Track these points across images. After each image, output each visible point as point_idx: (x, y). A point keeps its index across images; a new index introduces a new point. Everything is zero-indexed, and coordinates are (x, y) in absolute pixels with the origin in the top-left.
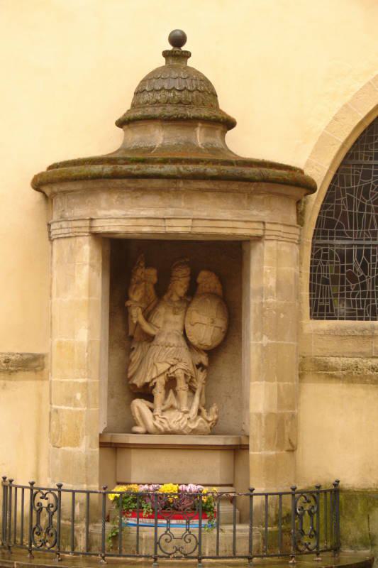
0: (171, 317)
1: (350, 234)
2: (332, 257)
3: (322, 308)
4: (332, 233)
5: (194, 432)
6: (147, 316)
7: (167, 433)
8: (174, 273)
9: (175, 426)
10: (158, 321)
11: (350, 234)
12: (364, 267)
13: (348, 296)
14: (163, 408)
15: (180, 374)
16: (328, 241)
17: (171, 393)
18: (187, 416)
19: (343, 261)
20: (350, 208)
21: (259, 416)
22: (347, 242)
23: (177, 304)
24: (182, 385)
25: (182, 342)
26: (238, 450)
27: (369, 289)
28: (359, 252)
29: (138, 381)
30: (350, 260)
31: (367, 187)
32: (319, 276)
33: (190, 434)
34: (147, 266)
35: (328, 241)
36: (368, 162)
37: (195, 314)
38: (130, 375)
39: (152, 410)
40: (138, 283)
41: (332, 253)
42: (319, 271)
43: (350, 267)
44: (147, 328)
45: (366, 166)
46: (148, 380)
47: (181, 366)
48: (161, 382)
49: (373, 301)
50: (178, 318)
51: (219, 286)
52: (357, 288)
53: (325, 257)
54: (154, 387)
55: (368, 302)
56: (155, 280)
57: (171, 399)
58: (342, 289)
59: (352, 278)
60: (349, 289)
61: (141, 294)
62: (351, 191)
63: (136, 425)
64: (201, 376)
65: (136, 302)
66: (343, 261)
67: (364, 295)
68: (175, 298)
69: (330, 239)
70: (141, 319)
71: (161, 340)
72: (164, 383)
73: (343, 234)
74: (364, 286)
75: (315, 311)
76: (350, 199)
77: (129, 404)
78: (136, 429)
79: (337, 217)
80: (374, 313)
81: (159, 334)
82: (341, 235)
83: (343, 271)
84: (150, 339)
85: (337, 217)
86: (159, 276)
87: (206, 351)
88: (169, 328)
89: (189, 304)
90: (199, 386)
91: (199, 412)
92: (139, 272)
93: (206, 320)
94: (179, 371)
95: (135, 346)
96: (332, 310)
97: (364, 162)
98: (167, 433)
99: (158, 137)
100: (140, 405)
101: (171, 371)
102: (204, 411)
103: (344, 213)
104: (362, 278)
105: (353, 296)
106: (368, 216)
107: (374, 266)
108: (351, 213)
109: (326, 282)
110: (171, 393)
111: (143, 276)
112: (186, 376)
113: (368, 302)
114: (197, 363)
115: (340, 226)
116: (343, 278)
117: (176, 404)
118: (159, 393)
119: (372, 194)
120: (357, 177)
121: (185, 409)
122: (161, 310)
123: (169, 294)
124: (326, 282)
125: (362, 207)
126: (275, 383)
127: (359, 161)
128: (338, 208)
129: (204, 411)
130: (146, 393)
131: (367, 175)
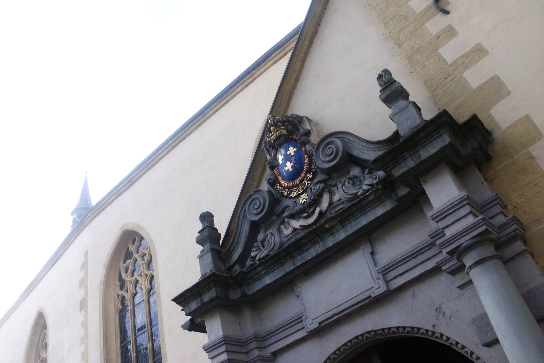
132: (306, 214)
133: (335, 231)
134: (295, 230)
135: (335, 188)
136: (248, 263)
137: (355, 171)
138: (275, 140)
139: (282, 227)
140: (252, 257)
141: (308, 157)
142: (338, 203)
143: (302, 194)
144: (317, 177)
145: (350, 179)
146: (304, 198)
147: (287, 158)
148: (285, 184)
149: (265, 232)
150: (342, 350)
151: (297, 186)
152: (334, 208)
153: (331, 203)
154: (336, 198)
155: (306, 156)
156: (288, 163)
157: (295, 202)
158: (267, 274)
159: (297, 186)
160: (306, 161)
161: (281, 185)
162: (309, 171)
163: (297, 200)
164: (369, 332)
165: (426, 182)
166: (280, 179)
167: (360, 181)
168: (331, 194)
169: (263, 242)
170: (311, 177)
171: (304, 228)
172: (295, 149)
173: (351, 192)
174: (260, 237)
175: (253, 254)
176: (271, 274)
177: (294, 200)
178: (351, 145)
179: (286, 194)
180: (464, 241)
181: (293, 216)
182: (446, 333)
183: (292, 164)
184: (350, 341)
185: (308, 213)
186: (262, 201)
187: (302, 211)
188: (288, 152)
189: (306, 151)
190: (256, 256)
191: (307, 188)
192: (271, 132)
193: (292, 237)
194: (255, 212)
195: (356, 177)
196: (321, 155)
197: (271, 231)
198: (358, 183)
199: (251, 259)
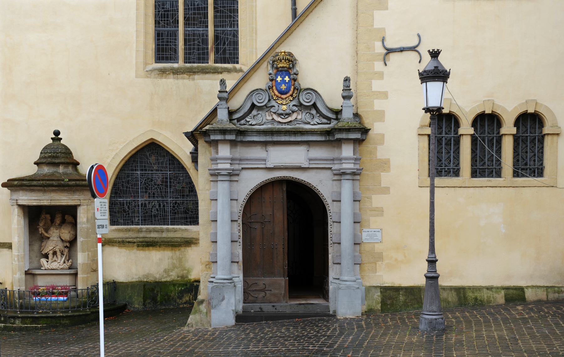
0: (55, 231)
1: (123, 196)
2: (117, 205)
3: (114, 222)
4: (117, 196)
5: (62, 269)
6: (47, 231)
7: (52, 269)
8: (56, 216)
9: (54, 267)
10: (51, 232)
11: (123, 196)
12: (129, 208)
13: (123, 217)
14: (52, 261)
15: (57, 250)
16: (116, 199)
17: (55, 256)
18: (59, 264)
19: (121, 206)
20: (123, 188)
21: (80, 264)
22: (122, 199)
23: (57, 227)
24: (59, 254)
25: (59, 239)
26: (76, 275)
27: (130, 215)
28: (127, 202)
29: (43, 252)
30: (123, 205)
31: (128, 181)
32: (113, 211)
33: (60, 269)
34: (46, 214)
35: (116, 199)
36: (129, 172)
37: (62, 230)
38: (41, 250)
39: (47, 262)
40: (42, 220)
41: (117, 203)
42: (113, 209)
43: (124, 208)
44: (46, 234)
45: (128, 173)
46: (46, 252)
47: (58, 247)
48: (51, 252)
49: (132, 219)
50: (58, 231)
51: (73, 220)
52: (126, 215)
53: (115, 204)
54: (49, 254)
55: (130, 219)
56: (50, 218)
57: (55, 258)
58: (121, 215)
59: (124, 211)
60: (123, 215)
61: (43, 223)
62: (123, 182)
63: (42, 267)
64: (67, 250)
65: (41, 226)
66: (121, 206)
67: (129, 217)
68: (57, 224)
69: (117, 198)
70: (43, 232)
71: (51, 238)
72: (52, 253)
73: (121, 196)
74: (129, 214)
75: (112, 222)
76: (123, 185)
77: (40, 260)
78: (42, 268)
79: (118, 191)
80: (133, 223)
81: (51, 237)
82: (120, 197)
83: (121, 209)
84: (48, 238)
85: (118, 191)
86: (51, 217)
87: (68, 242)
88: (54, 235)
89: (62, 225)
90: (65, 253)
91: (64, 262)
92: (43, 216)
93: (67, 232)
94: (57, 249)
95: (44, 240)
96: (118, 222)
97: (127, 172)
98: (52, 269)
99: (46, 170)
100: (43, 261)
101: (54, 249)
102: (66, 262)
103: (121, 189)
104: (128, 211)
105: (125, 217)
106: (129, 190)
107: (132, 207)
108: (123, 190)
109: (115, 213)
110: (55, 256)
111: (44, 217)
112: (60, 250)
113: (130, 219)
114: (65, 246)
115: (120, 194)
116: (121, 211)
117: (56, 260)
118: (50, 256)
119: (130, 183)
120: (125, 177)
121: (58, 261)
122: (52, 228)
123: (54, 223)
124: (115, 213)
125: (127, 187)
126: (87, 253)
127: (125, 172)
128: (119, 188)
129: (66, 262)
130: (46, 256)
131: (128, 176)
132: (283, 117)
133: (297, 135)
134: (273, 119)
135: (300, 113)
136: (243, 122)
137: (314, 112)
138: (281, 67)
139: (267, 113)
140: (246, 120)
141: (294, 88)
142: (300, 120)
143: (284, 105)
144: (294, 101)
145: (310, 113)
146: (284, 107)
147: (283, 81)
148: (277, 93)
149: (257, 111)
150: (275, 178)
151: (283, 99)
152: (297, 121)
153: (296, 118)
154: (299, 117)
155: (293, 87)
156: (283, 85)
157: (279, 106)
158: (256, 136)
159: (283, 99)
160: (292, 89)
161: (273, 91)
162: (292, 95)
163: (280, 106)
164: (290, 177)
165: (344, 144)
166: (274, 88)
167: (314, 117)
168: (298, 114)
169: (254, 116)
170: (292, 99)
171: (280, 122)
172: (289, 79)
173: (308, 121)
174: (254, 112)
175: (248, 120)
176: (258, 137)
177: (278, 105)
178: (318, 100)
179: (274, 98)
180: (348, 171)
181: (275, 113)
182: (319, 189)
183: (285, 87)
184: (281, 177)
185: (284, 117)
186: (264, 98)
187: (282, 114)
188: (285, 79)
189: (294, 84)
190: (250, 121)
191: (288, 103)
192: (281, 62)
193: (270, 122)
194: (259, 101)
195: (312, 114)
196: (304, 95)
197: (260, 112)
198: (312, 117)
199: (245, 121)
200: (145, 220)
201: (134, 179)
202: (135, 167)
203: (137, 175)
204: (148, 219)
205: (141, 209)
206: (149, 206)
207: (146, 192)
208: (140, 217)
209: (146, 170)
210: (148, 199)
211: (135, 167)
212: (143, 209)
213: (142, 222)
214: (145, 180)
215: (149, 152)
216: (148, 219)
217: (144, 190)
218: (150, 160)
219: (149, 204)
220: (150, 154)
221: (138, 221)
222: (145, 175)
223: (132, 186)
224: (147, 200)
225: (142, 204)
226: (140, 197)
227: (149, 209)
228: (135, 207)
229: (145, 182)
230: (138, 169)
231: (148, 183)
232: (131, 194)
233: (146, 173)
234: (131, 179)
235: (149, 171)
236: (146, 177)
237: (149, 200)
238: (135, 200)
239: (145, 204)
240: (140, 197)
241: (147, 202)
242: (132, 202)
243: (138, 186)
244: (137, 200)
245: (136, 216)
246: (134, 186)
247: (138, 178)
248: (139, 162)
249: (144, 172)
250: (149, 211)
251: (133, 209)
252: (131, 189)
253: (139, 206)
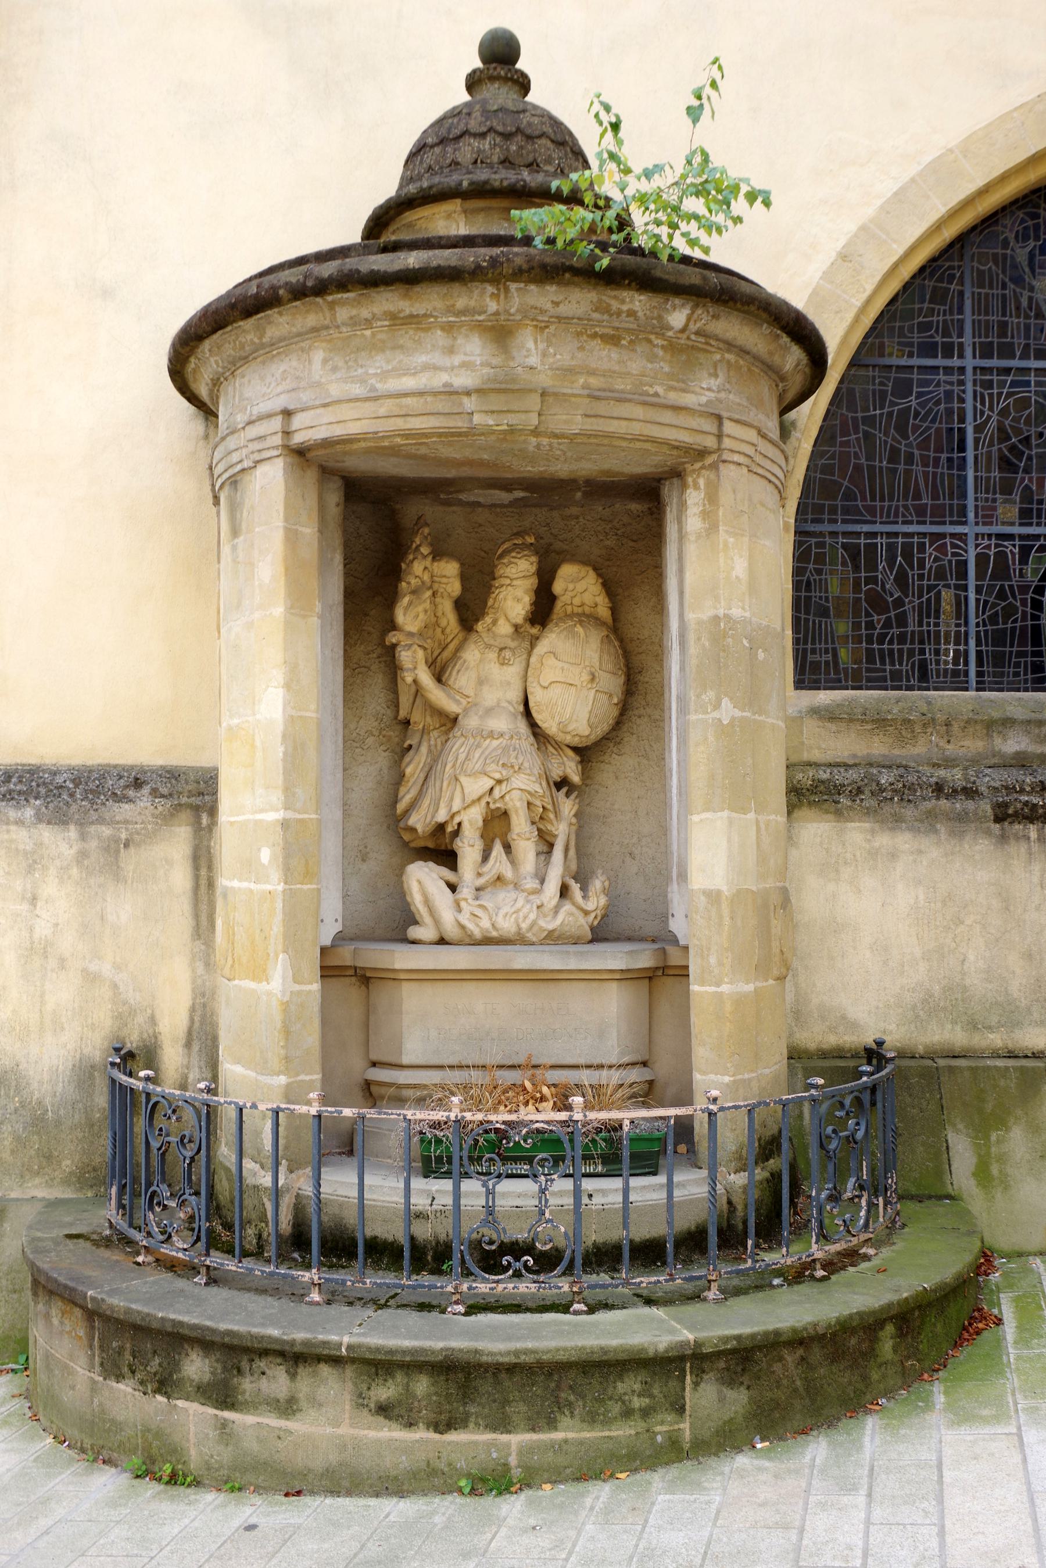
1: (872, 511)
3: (815, 667)
4: (833, 510)
12: (901, 580)
15: (516, 804)
16: (826, 527)
17: (498, 849)
27: (912, 627)
28: (891, 548)
30: (872, 566)
43: (874, 580)
49: (922, 652)
52: (888, 624)
55: (911, 653)
59: (877, 602)
60: (870, 625)
62: (870, 421)
74: (902, 620)
103: (858, 468)
104: (899, 603)
107: (921, 577)
108: (872, 468)
110: (498, 849)
113: (911, 653)
120: (883, 395)
131: (903, 389)
200: (999, 660)
201: (938, 403)
202: (946, 333)
203: (955, 378)
204: (1020, 654)
205: (979, 590)
206: (1021, 575)
207: (1007, 489)
208: (972, 643)
209: (1007, 352)
210: (1016, 530)
211: (946, 333)
212: (989, 593)
213: (980, 674)
214: (1004, 412)
215: (1026, 238)
216: (1020, 654)
217: (996, 474)
218: (1032, 289)
219: (1024, 559)
220: (1031, 256)
221: (956, 662)
222: (1002, 384)
223: (924, 445)
224: (1010, 537)
225: (982, 560)
226: (971, 515)
227: (1024, 589)
228: (941, 575)
229: (1001, 429)
230: (961, 346)
231: (1018, 431)
232: (917, 496)
233: (1007, 371)
234: (922, 405)
235: (1025, 356)
236: (1009, 395)
237: (1022, 537)
238: (942, 536)
239: (1001, 556)
240: (971, 515)
241: (1012, 549)
242: (922, 547)
243: (962, 448)
244: (953, 535)
245: (947, 634)
246: (939, 450)
247: (962, 400)
248: (968, 303)
249: (995, 362)
250: (1024, 602)
251: (930, 588)
252: (917, 468)
253: (963, 574)
